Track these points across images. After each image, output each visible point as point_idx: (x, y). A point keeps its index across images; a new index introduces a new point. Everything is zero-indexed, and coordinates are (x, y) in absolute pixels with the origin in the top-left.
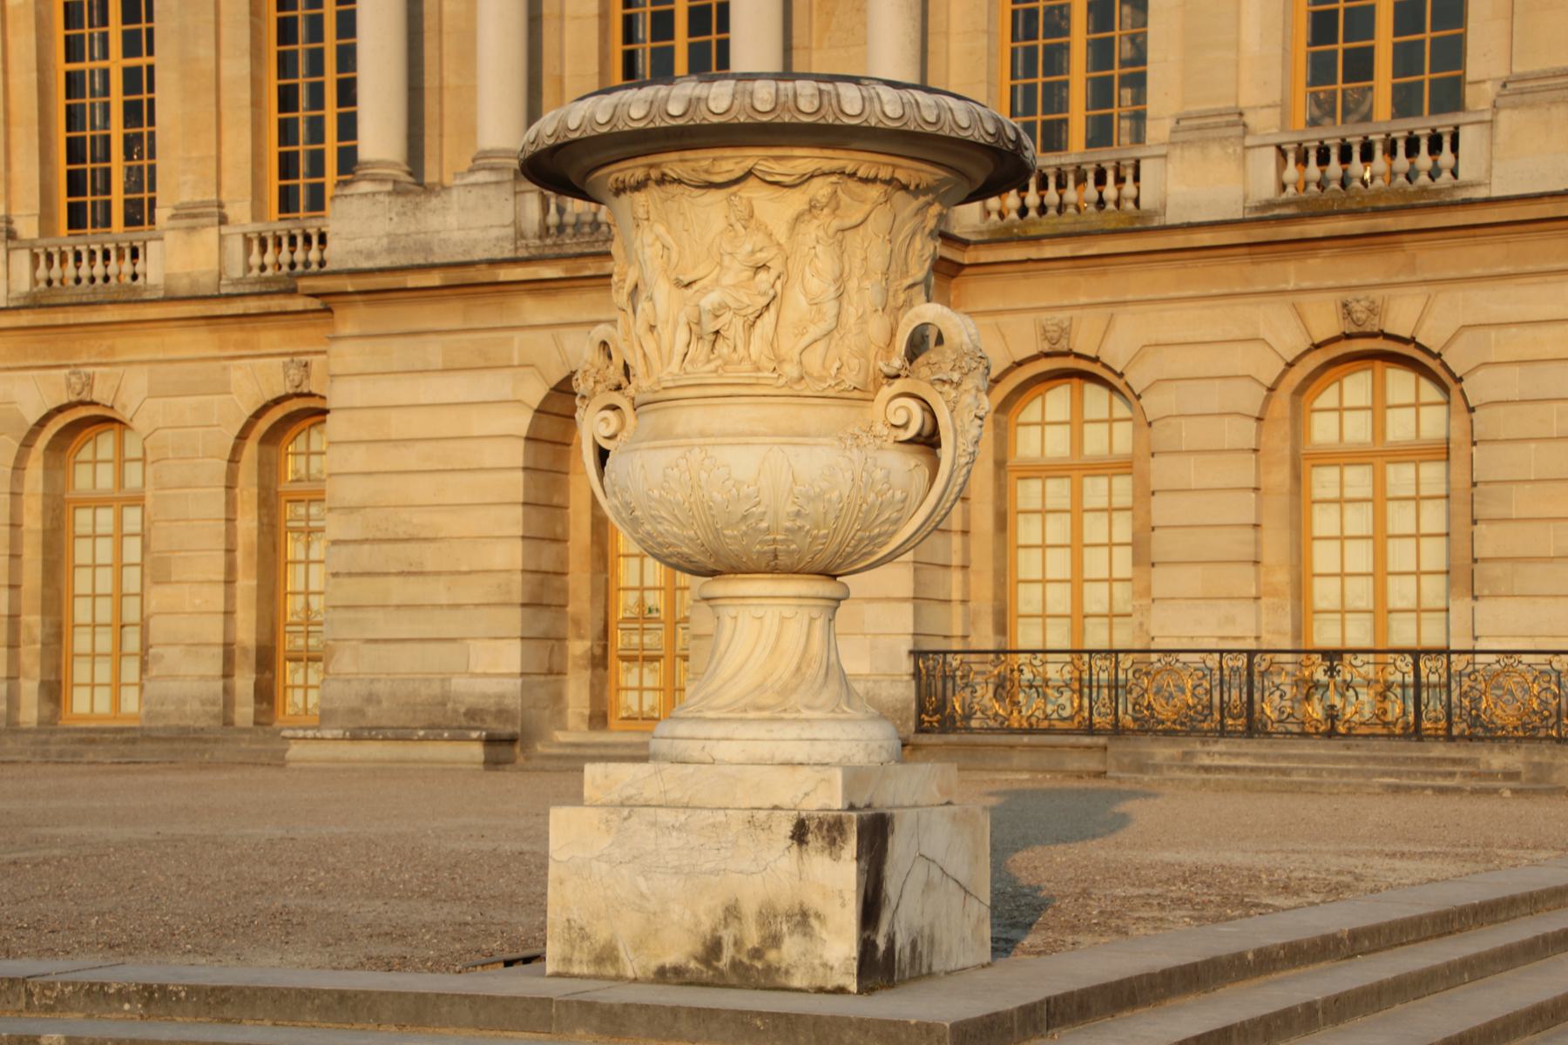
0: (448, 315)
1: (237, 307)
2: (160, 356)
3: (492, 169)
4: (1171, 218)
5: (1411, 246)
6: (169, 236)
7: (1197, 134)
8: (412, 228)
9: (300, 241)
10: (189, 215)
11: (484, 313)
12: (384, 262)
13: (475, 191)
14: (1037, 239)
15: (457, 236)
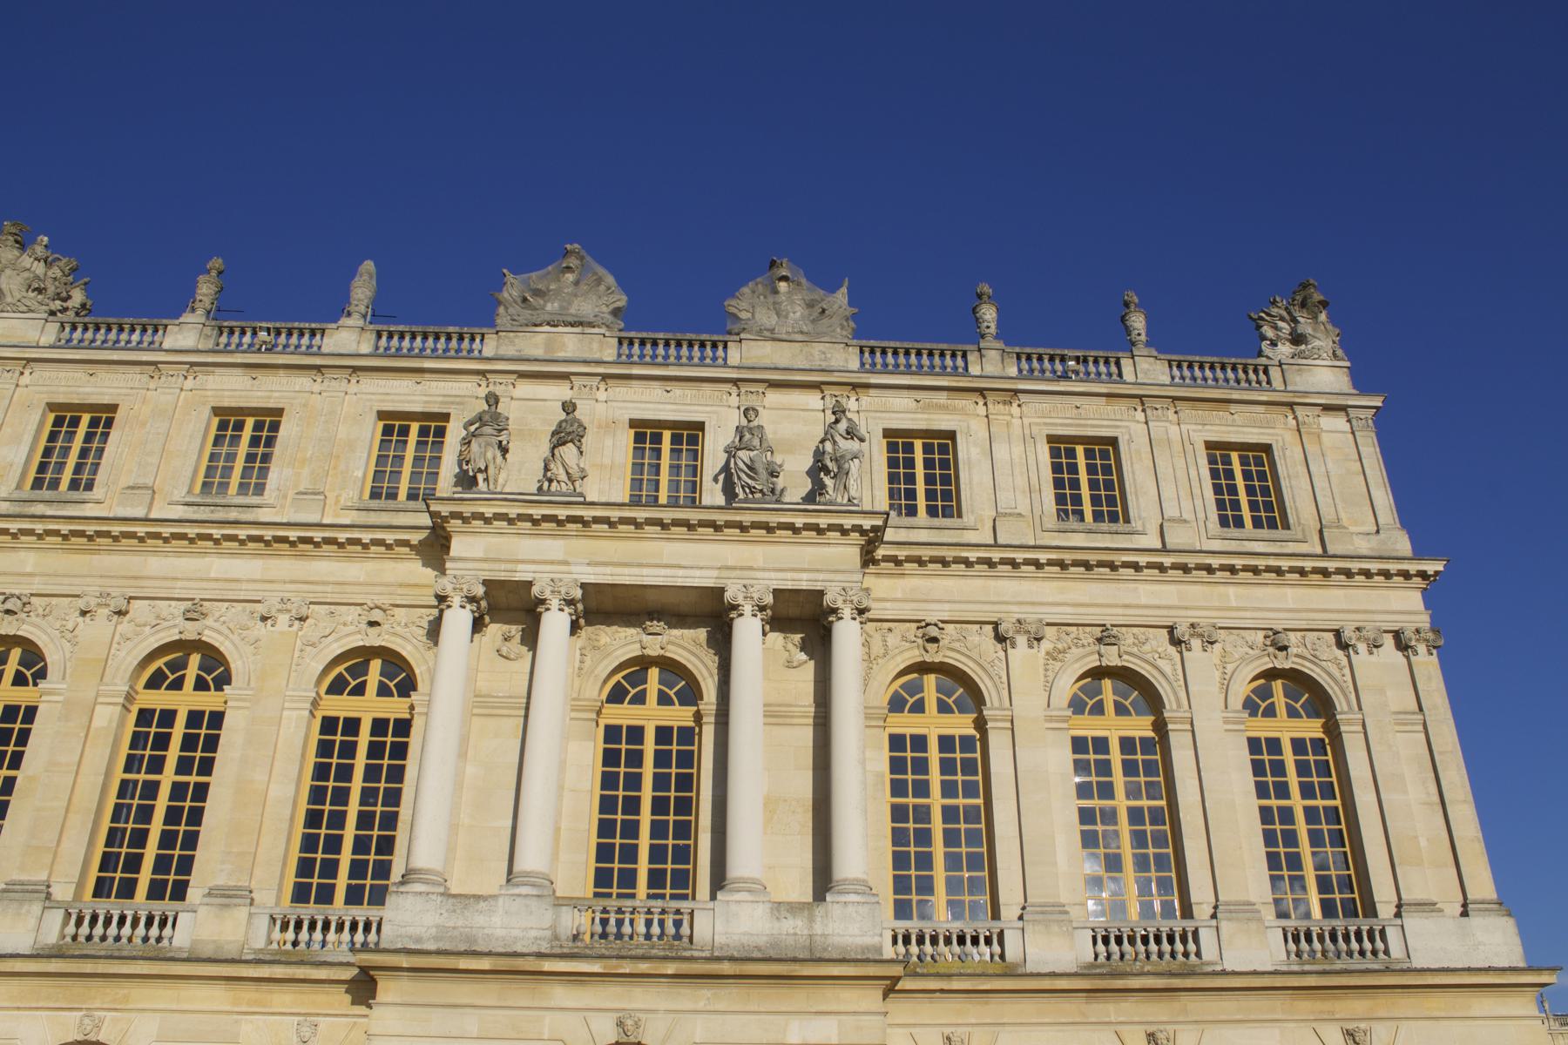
0: (489, 992)
1: (264, 971)
2: (174, 1007)
3: (533, 885)
4: (1030, 968)
5: (1185, 998)
6: (202, 911)
7: (1040, 917)
8: (460, 923)
9: (319, 925)
10: (225, 896)
11: (518, 993)
12: (432, 946)
13: (519, 900)
14: (949, 976)
15: (499, 932)
